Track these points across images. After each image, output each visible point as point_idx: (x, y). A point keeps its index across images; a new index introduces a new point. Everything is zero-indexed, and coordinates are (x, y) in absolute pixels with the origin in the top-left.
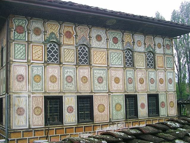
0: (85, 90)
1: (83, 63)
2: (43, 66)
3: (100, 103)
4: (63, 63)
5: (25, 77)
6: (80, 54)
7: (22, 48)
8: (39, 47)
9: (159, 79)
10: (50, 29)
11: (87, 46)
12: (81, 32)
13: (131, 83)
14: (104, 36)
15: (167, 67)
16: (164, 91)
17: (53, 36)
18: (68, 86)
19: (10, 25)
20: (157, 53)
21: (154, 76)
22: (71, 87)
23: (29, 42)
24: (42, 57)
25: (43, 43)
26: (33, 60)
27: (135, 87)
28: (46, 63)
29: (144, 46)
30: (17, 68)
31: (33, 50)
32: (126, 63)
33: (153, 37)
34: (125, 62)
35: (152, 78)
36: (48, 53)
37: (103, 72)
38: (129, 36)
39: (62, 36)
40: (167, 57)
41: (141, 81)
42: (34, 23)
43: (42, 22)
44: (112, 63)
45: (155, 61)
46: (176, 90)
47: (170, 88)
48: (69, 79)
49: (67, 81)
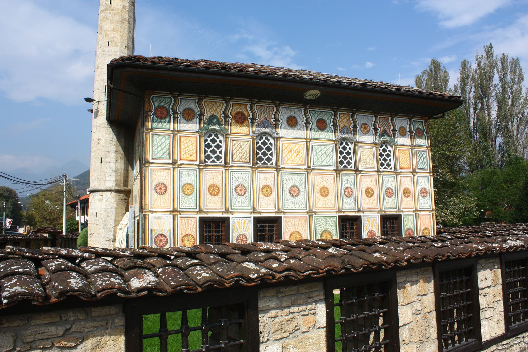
0: (267, 207)
1: (265, 163)
2: (198, 170)
4: (231, 164)
5: (168, 186)
6: (260, 148)
8: (192, 138)
9: (403, 189)
11: (271, 136)
13: (350, 197)
14: (301, 117)
16: (412, 210)
17: (215, 120)
18: (239, 202)
19: (147, 106)
20: (397, 145)
21: (393, 184)
23: (175, 132)
25: (197, 132)
27: (356, 202)
28: (202, 165)
29: (374, 133)
30: (156, 173)
31: (182, 144)
32: (342, 163)
33: (390, 118)
34: (339, 160)
36: (206, 149)
37: (299, 177)
38: (346, 116)
40: (416, 151)
41: (369, 193)
42: (183, 102)
43: (197, 99)
44: (316, 164)
45: (395, 159)
46: (434, 207)
47: (422, 206)
48: (241, 190)
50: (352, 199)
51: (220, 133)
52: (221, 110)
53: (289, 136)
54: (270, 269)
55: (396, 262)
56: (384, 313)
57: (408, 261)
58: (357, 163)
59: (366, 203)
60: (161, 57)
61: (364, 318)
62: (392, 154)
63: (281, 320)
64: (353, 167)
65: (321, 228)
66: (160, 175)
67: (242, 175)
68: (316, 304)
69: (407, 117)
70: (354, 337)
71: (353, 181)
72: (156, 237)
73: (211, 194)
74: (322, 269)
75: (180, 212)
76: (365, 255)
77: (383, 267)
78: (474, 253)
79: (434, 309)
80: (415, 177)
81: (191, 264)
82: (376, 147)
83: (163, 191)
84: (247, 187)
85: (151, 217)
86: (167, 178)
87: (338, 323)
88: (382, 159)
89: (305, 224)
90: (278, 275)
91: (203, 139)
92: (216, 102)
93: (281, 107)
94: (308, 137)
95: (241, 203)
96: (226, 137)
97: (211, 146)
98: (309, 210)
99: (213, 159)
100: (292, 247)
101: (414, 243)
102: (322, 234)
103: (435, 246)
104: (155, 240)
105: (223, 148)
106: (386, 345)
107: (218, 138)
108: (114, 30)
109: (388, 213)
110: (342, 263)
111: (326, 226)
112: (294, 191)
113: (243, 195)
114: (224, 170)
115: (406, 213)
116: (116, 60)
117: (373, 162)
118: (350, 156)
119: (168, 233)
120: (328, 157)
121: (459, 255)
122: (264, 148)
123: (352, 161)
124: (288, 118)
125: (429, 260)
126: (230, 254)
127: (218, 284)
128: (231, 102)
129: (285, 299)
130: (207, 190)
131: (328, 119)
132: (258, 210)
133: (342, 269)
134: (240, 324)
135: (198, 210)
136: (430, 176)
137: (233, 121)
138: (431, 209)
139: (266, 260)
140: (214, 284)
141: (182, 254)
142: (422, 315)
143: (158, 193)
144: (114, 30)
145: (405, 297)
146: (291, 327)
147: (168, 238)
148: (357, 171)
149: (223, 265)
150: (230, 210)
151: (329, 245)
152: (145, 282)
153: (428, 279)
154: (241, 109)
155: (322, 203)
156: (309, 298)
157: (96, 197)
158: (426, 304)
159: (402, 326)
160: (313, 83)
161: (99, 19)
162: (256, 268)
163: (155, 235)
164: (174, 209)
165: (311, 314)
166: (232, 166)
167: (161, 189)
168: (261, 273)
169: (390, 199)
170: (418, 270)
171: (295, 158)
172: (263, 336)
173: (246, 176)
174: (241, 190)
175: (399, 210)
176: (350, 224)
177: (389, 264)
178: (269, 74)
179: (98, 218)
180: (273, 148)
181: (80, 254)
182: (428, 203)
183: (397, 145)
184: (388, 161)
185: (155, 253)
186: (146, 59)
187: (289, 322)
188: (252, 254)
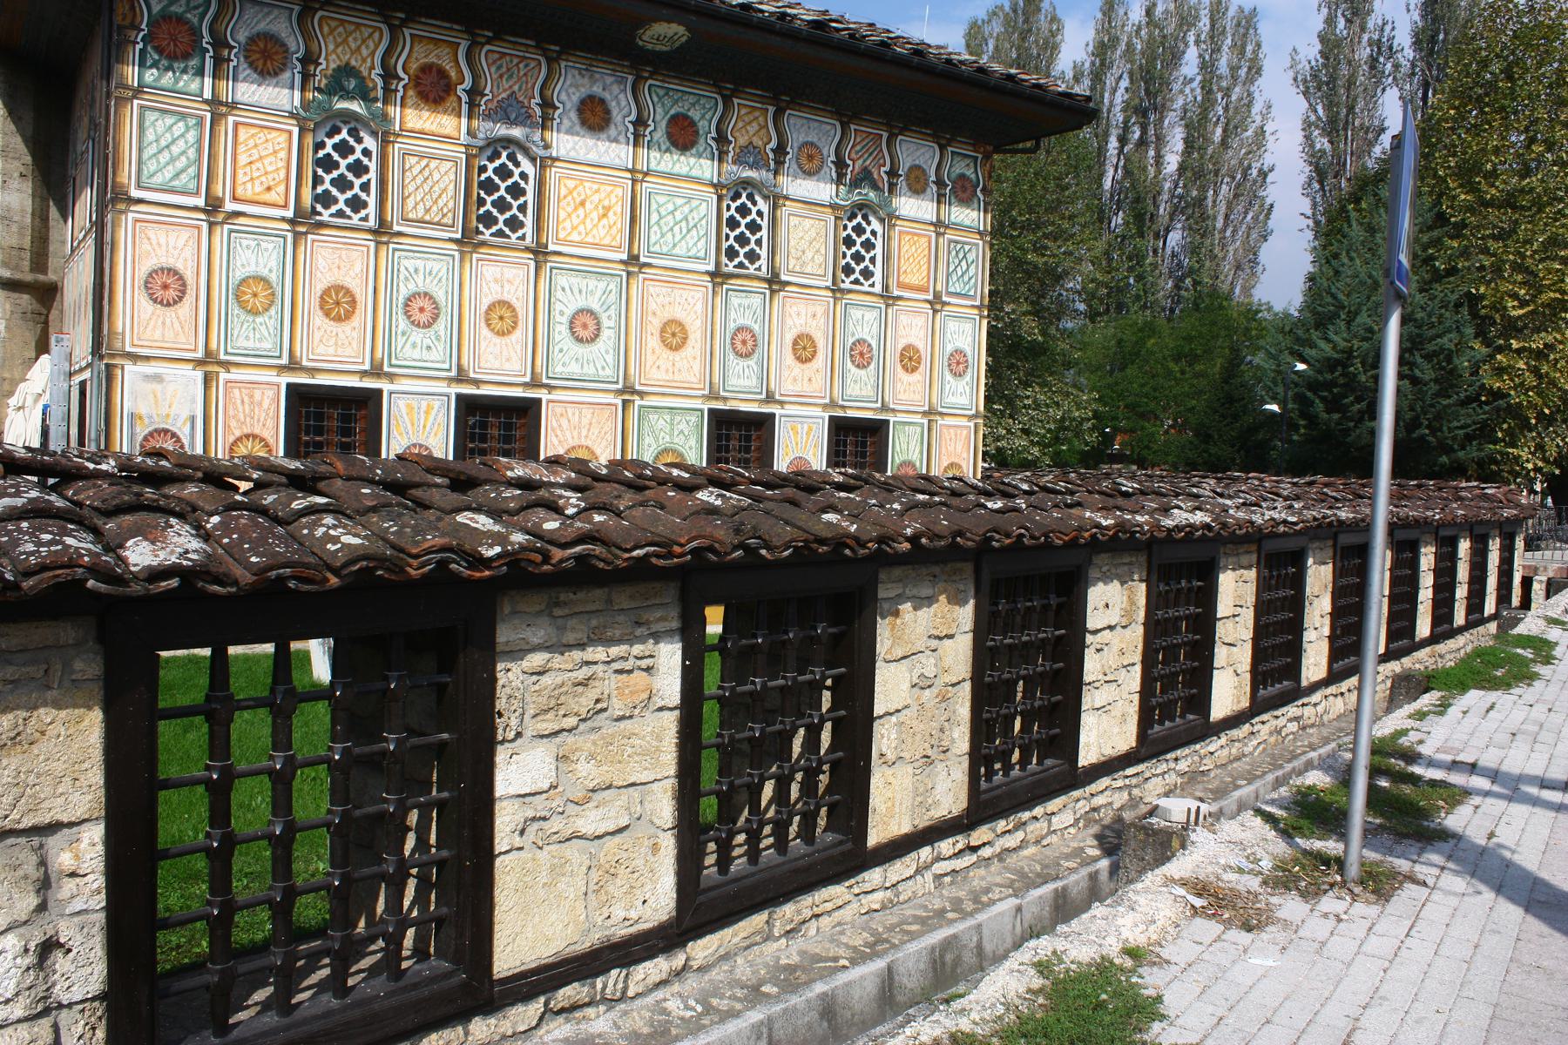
0: (501, 368)
1: (500, 233)
2: (290, 235)
3: (576, 442)
4: (396, 228)
6: (489, 186)
7: (182, 135)
8: (274, 134)
9: (900, 347)
10: (337, 46)
12: (501, 76)
13: (748, 355)
14: (624, 103)
18: (414, 345)
20: (898, 218)
23: (219, 108)
25: (292, 115)
26: (235, 199)
28: (304, 222)
29: (834, 175)
30: (151, 234)
31: (241, 148)
32: (731, 254)
33: (885, 135)
34: (725, 245)
35: (859, 341)
36: (320, 172)
38: (757, 114)
39: (400, 87)
40: (950, 241)
41: (804, 349)
44: (656, 248)
45: (887, 258)
46: (982, 408)
47: (951, 400)
48: (421, 310)
49: (409, 317)
50: (752, 362)
51: (366, 125)
52: (373, 53)
54: (537, 534)
55: (881, 540)
56: (836, 679)
57: (913, 540)
58: (777, 258)
59: (793, 378)
61: (782, 688)
62: (879, 243)
63: (559, 680)
64: (764, 269)
65: (656, 439)
66: (163, 241)
67: (429, 264)
68: (657, 643)
69: (935, 137)
70: (751, 740)
71: (759, 312)
73: (327, 314)
74: (682, 545)
75: (226, 365)
76: (801, 517)
77: (847, 552)
78: (1086, 535)
79: (968, 675)
80: (938, 316)
81: (306, 508)
82: (837, 218)
83: (172, 294)
85: (131, 370)
86: (189, 252)
87: (711, 698)
88: (849, 253)
89: (609, 425)
90: (558, 554)
91: (309, 140)
92: (358, 25)
93: (563, 64)
94: (639, 167)
95: (420, 349)
96: (385, 140)
97: (336, 165)
98: (625, 387)
99: (341, 205)
100: (597, 478)
101: (932, 494)
103: (985, 507)
105: (372, 175)
106: (835, 766)
109: (851, 414)
110: (737, 531)
111: (671, 435)
112: (585, 326)
113: (428, 325)
114: (372, 244)
115: (901, 417)
118: (758, 235)
119: (187, 429)
120: (694, 232)
121: (1047, 537)
122: (503, 186)
124: (583, 102)
126: (417, 485)
127: (387, 569)
128: (407, 32)
129: (572, 622)
130: (316, 302)
131: (703, 117)
132: (472, 375)
133: (736, 548)
134: (441, 689)
135: (285, 361)
136: (981, 317)
137: (411, 93)
139: (523, 509)
140: (376, 568)
141: (276, 478)
142: (935, 690)
143: (155, 301)
145: (896, 639)
146: (585, 702)
148: (774, 282)
149: (400, 515)
150: (386, 369)
151: (702, 480)
152: (172, 552)
153: (961, 596)
154: (438, 57)
155: (663, 367)
156: (638, 624)
158: (948, 662)
159: (880, 717)
162: (497, 528)
163: (141, 432)
164: (208, 353)
165: (640, 668)
166: (400, 234)
167: (166, 287)
168: (512, 544)
169: (863, 372)
170: (936, 569)
172: (506, 725)
173: (439, 266)
174: (422, 310)
175: (885, 408)
176: (740, 434)
177: (863, 546)
180: (530, 188)
183: (898, 218)
184: (867, 262)
185: (196, 469)
187: (580, 689)
188: (481, 490)
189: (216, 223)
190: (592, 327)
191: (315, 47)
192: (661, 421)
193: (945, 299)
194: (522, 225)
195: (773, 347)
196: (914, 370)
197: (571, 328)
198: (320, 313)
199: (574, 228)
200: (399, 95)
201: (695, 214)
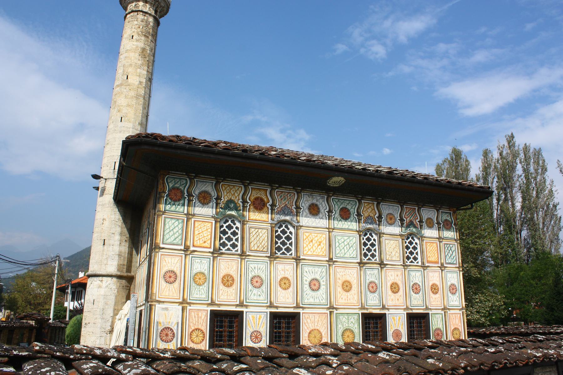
0: (285, 302)
1: (283, 253)
2: (212, 258)
3: (313, 328)
4: (248, 253)
6: (279, 237)
8: (207, 223)
11: (291, 224)
13: (374, 292)
14: (324, 205)
15: (447, 263)
18: (254, 295)
19: (160, 187)
20: (425, 237)
22: (260, 295)
23: (189, 216)
24: (209, 241)
25: (213, 217)
27: (381, 299)
28: (216, 253)
29: (400, 224)
30: (166, 259)
31: (196, 229)
32: (366, 255)
33: (417, 208)
34: (363, 252)
35: (415, 284)
36: (222, 235)
37: (320, 270)
38: (370, 205)
40: (445, 244)
41: (395, 288)
42: (200, 184)
43: (214, 182)
44: (339, 255)
45: (422, 252)
46: (464, 306)
47: (451, 303)
48: (257, 282)
49: (252, 285)
51: (237, 219)
52: (239, 195)
53: (310, 225)
55: (453, 369)
57: (465, 368)
60: (178, 136)
62: (418, 247)
64: (378, 260)
65: (343, 325)
66: (170, 261)
71: (377, 276)
72: (162, 331)
73: (224, 285)
75: (190, 304)
76: (420, 361)
78: (532, 361)
80: (443, 272)
81: (239, 370)
83: (172, 279)
84: (264, 279)
85: (158, 308)
86: (178, 265)
88: (408, 252)
89: (325, 321)
91: (218, 225)
92: (234, 186)
93: (302, 194)
94: (331, 227)
95: (257, 296)
96: (243, 223)
97: (227, 233)
98: (330, 306)
99: (229, 246)
100: (342, 351)
102: (343, 332)
103: (488, 351)
104: (160, 334)
105: (239, 236)
107: (235, 224)
108: (128, 105)
109: (414, 311)
111: (348, 324)
112: (315, 285)
113: (259, 287)
114: (239, 259)
115: (434, 312)
116: (132, 136)
117: (398, 255)
118: (375, 248)
119: (176, 327)
120: (352, 248)
121: (516, 363)
122: (284, 237)
123: (377, 254)
124: (310, 206)
125: (486, 368)
126: (277, 358)
128: (250, 187)
130: (220, 281)
131: (352, 208)
132: (275, 305)
136: (460, 271)
137: (252, 207)
138: (461, 307)
139: (317, 366)
141: (226, 357)
143: (167, 282)
144: (128, 105)
147: (175, 332)
148: (382, 264)
149: (273, 371)
150: (245, 303)
151: (380, 349)
154: (260, 194)
155: (344, 298)
157: (95, 283)
160: (337, 170)
161: (114, 94)
163: (160, 328)
164: (184, 300)
166: (249, 255)
167: (171, 277)
169: (417, 295)
171: (317, 249)
173: (263, 266)
174: (257, 282)
175: (427, 308)
178: (292, 159)
179: (95, 306)
180: (293, 237)
181: (116, 355)
182: (457, 300)
183: (425, 237)
184: (415, 254)
185: (198, 355)
186: (163, 138)
189: (187, 255)
190: (317, 285)
191: (220, 194)
192: (344, 319)
193: (445, 265)
194: (291, 250)
195: (383, 288)
196: (436, 293)
197: (310, 286)
198: (222, 284)
199: (309, 250)
200: (248, 208)
201: (351, 242)
